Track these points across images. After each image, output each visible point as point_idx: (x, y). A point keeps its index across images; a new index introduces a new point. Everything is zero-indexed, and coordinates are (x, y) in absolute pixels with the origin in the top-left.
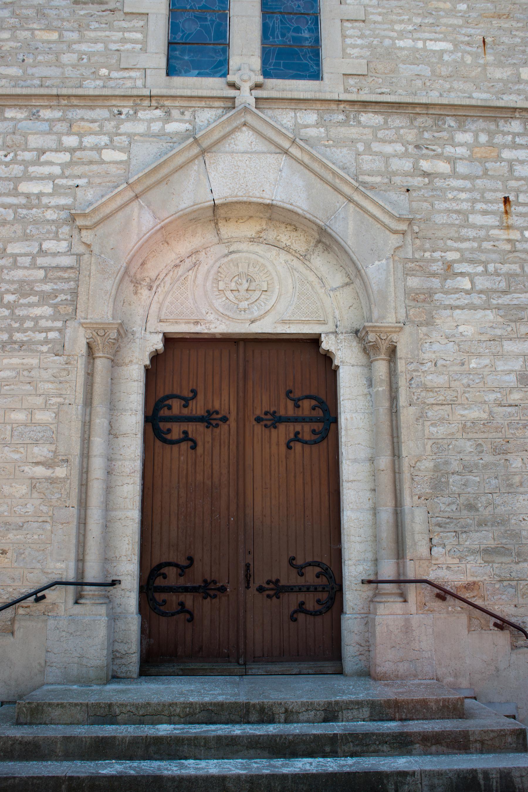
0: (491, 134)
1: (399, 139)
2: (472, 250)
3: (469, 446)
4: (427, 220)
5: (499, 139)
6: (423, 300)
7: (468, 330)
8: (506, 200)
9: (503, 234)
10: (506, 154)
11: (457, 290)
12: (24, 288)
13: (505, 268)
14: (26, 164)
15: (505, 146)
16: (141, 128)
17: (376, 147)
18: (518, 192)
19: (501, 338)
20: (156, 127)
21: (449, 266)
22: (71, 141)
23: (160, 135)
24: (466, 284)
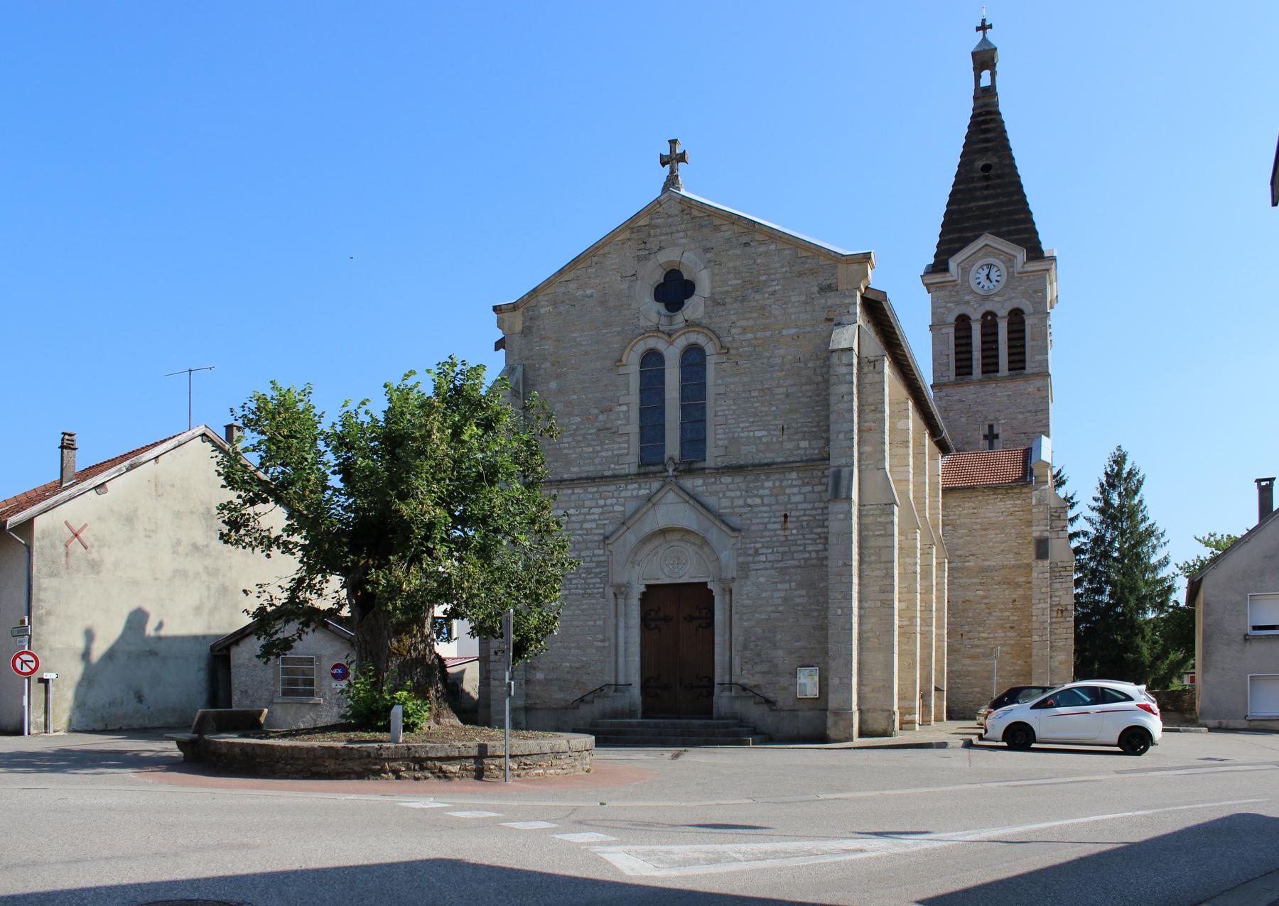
0: (781, 481)
1: (739, 489)
5: (785, 483)
6: (744, 569)
7: (762, 580)
8: (786, 516)
9: (782, 533)
10: (788, 491)
12: (589, 571)
13: (781, 549)
14: (585, 514)
16: (628, 494)
17: (728, 494)
18: (791, 510)
20: (635, 493)
21: (756, 551)
22: (601, 502)
23: (638, 497)
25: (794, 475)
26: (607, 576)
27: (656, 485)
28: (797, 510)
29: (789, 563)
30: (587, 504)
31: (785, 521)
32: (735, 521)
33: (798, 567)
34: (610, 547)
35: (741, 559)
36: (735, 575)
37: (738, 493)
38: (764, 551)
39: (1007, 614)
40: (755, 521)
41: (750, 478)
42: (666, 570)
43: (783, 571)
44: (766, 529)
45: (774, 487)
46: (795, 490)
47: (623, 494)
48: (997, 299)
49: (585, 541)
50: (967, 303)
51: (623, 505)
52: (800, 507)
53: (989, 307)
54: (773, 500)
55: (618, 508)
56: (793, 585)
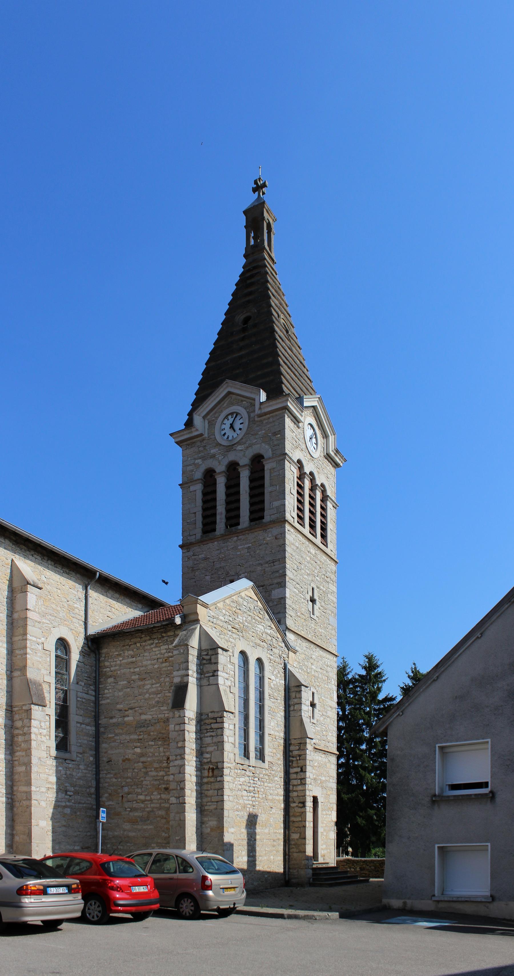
39: (162, 773)
48: (239, 448)
50: (213, 456)
53: (232, 457)
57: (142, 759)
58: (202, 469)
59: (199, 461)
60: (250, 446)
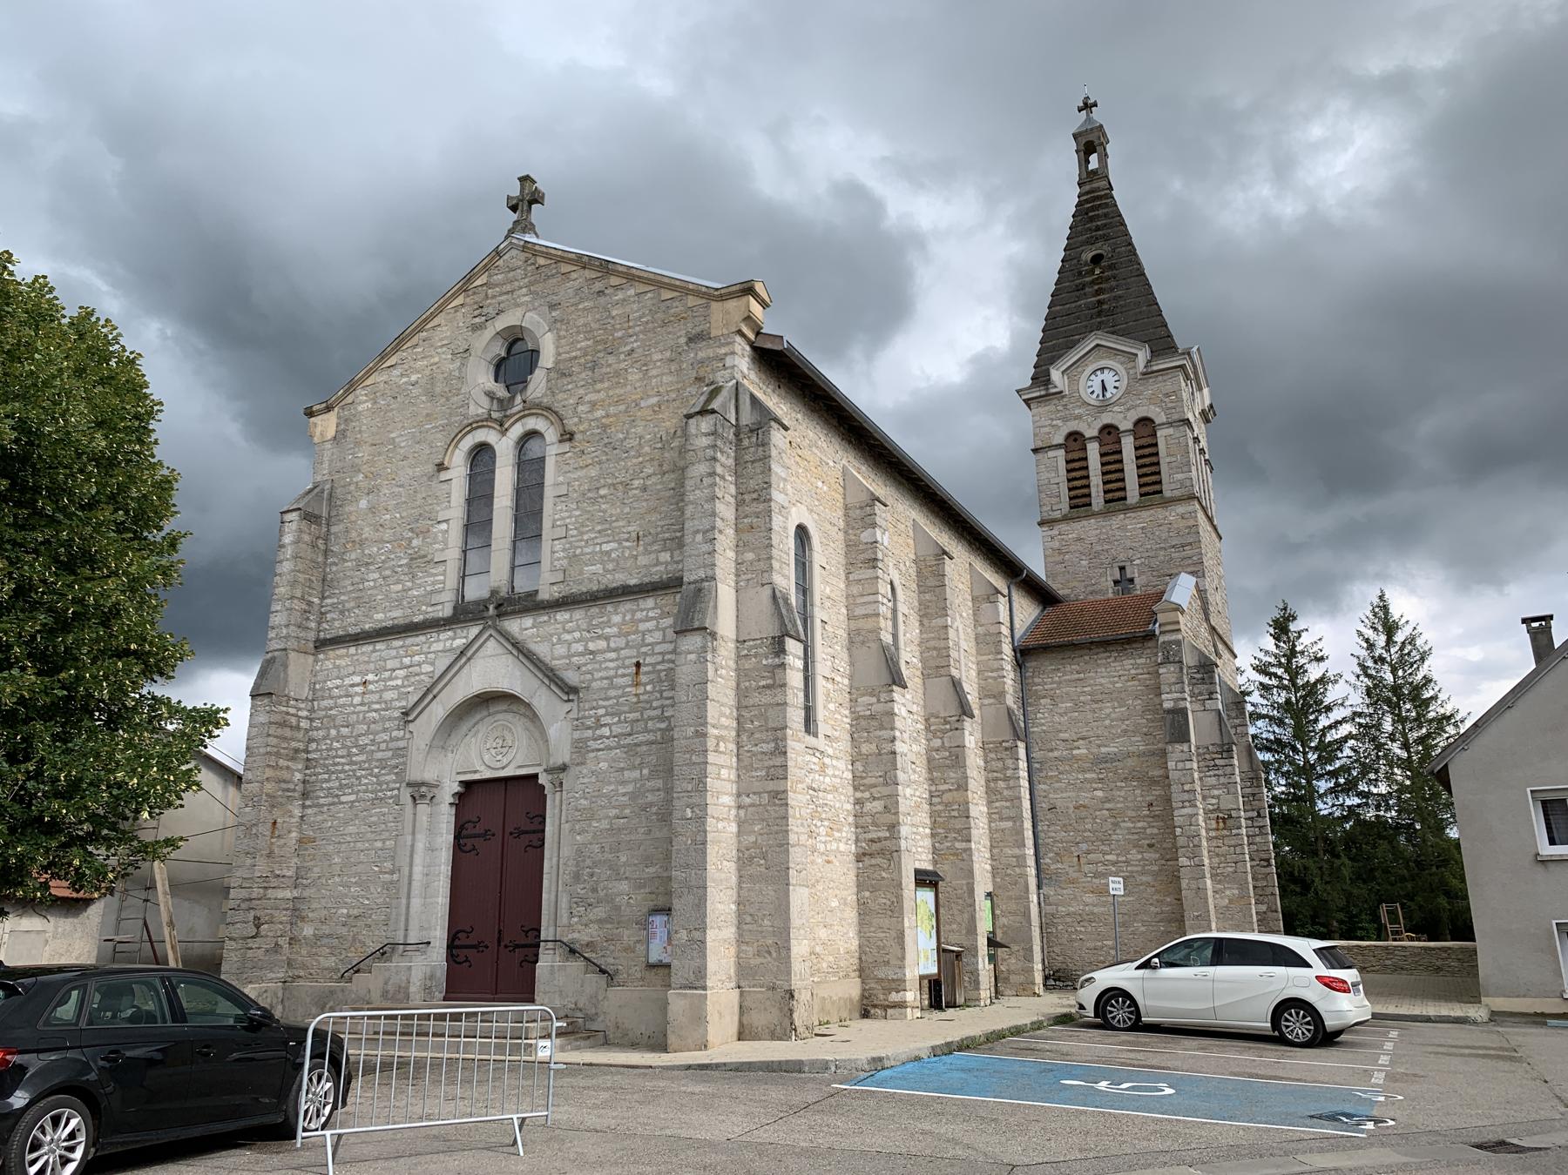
1: (578, 629)
2: (612, 706)
3: (596, 848)
4: (587, 688)
5: (639, 615)
6: (580, 747)
8: (638, 665)
10: (642, 626)
11: (601, 737)
14: (385, 680)
15: (641, 621)
16: (440, 646)
17: (567, 637)
19: (623, 769)
20: (448, 644)
22: (407, 661)
24: (606, 731)
25: (650, 602)
26: (403, 771)
27: (474, 631)
28: (653, 654)
29: (641, 738)
30: (390, 664)
31: (637, 673)
32: (572, 677)
33: (652, 743)
34: (411, 727)
35: (577, 735)
36: (567, 759)
37: (577, 635)
38: (607, 720)
40: (597, 675)
41: (595, 610)
42: (486, 757)
43: (631, 749)
44: (612, 686)
45: (624, 622)
46: (651, 625)
47: (435, 647)
49: (383, 719)
50: (1079, 417)
51: (432, 664)
52: (658, 649)
53: (1107, 419)
54: (621, 642)
55: (427, 668)
56: (645, 771)
57: (1108, 806)
58: (1065, 431)
59: (1059, 422)
60: (1134, 407)
